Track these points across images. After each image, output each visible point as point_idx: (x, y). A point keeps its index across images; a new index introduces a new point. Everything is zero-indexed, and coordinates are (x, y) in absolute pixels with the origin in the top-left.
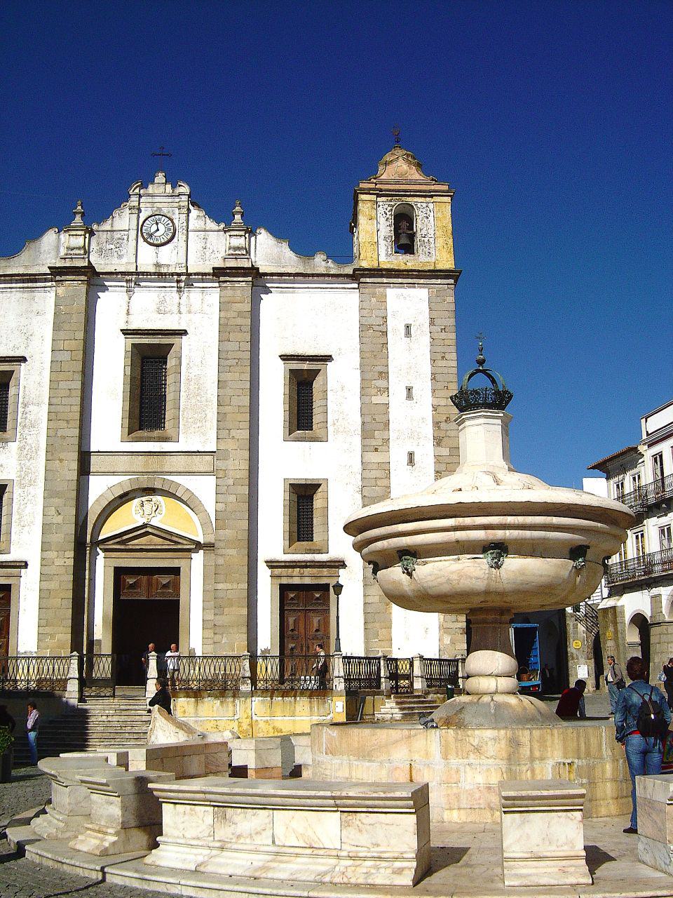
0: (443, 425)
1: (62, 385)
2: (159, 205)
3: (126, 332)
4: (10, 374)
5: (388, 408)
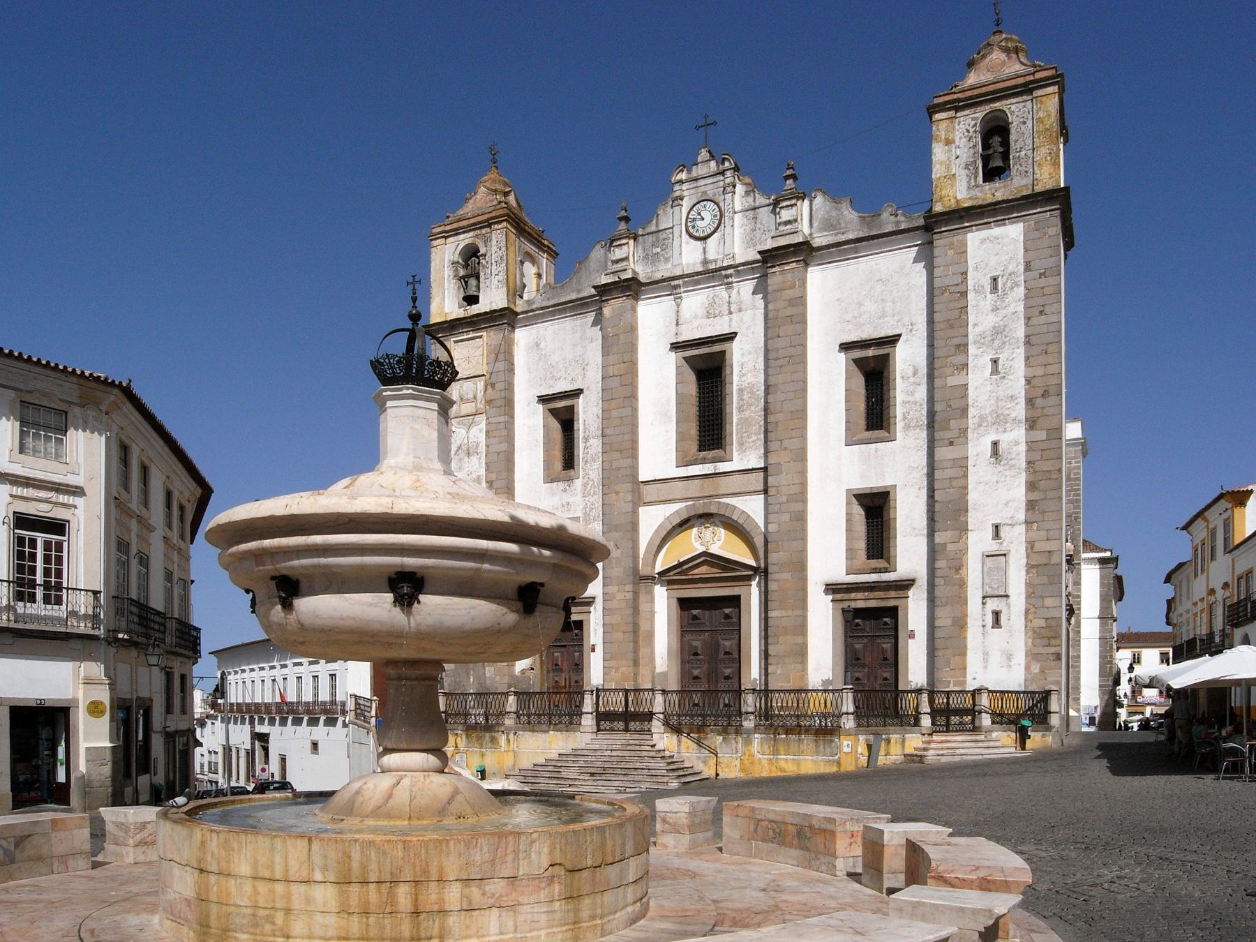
1: (615, 414)
2: (703, 189)
3: (676, 347)
4: (571, 410)
5: (967, 389)
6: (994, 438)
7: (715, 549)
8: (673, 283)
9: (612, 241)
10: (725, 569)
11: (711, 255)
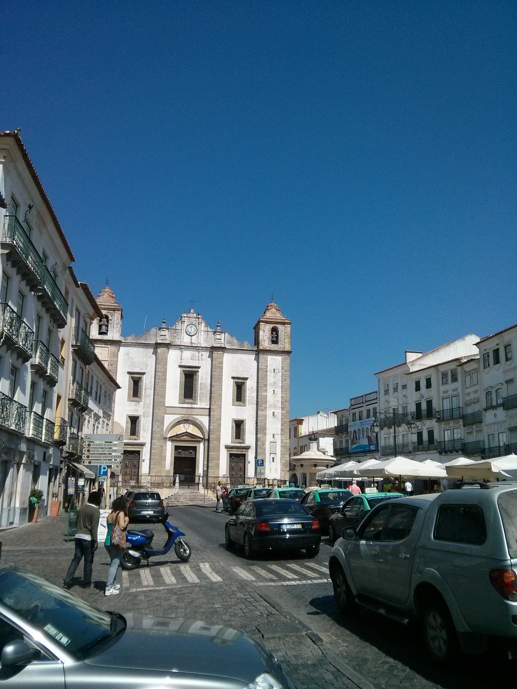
0: (284, 403)
2: (192, 321)
3: (180, 366)
6: (274, 411)
7: (189, 431)
8: (181, 347)
9: (161, 329)
10: (192, 438)
11: (193, 342)
